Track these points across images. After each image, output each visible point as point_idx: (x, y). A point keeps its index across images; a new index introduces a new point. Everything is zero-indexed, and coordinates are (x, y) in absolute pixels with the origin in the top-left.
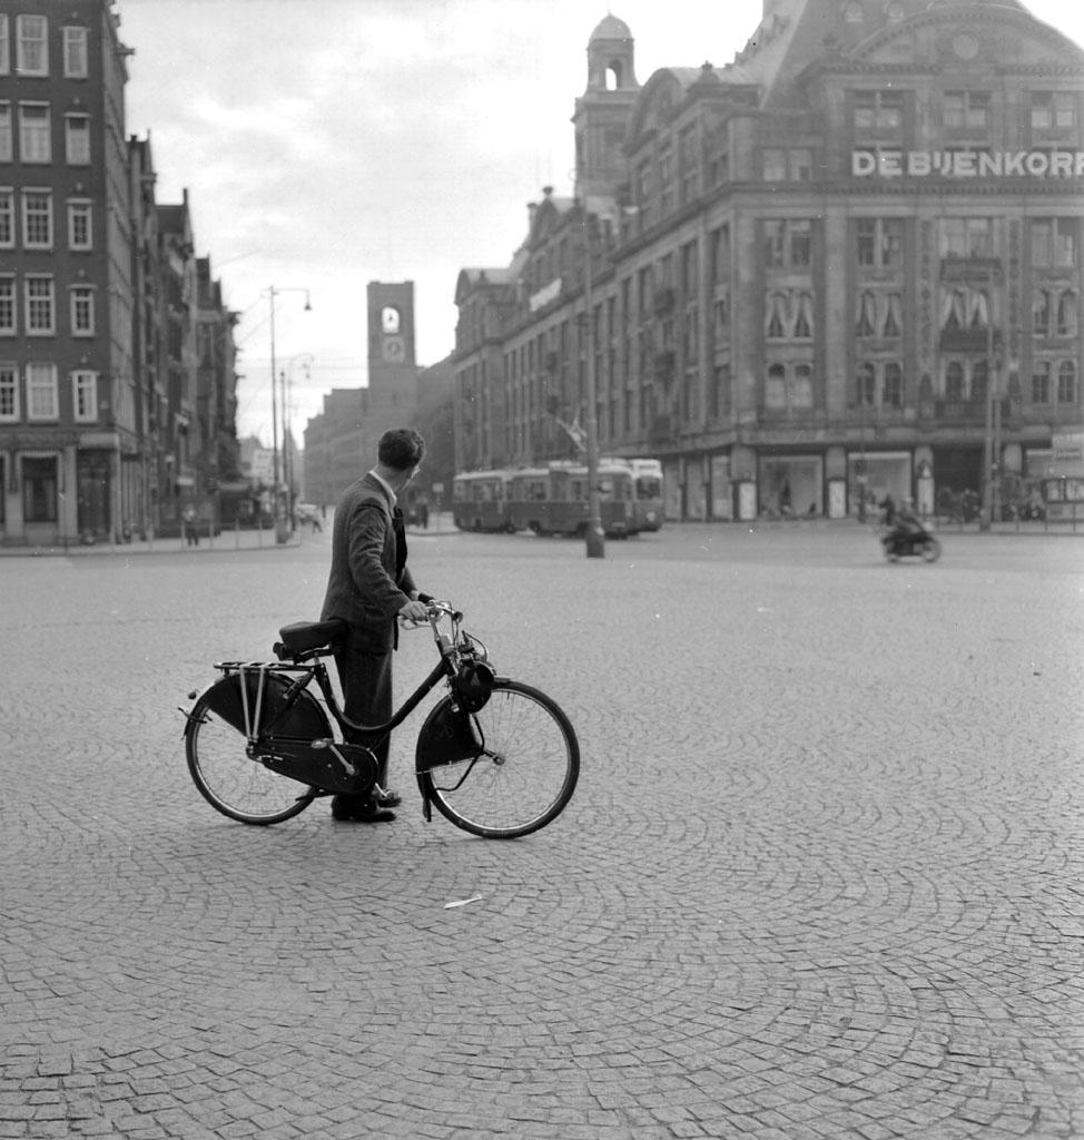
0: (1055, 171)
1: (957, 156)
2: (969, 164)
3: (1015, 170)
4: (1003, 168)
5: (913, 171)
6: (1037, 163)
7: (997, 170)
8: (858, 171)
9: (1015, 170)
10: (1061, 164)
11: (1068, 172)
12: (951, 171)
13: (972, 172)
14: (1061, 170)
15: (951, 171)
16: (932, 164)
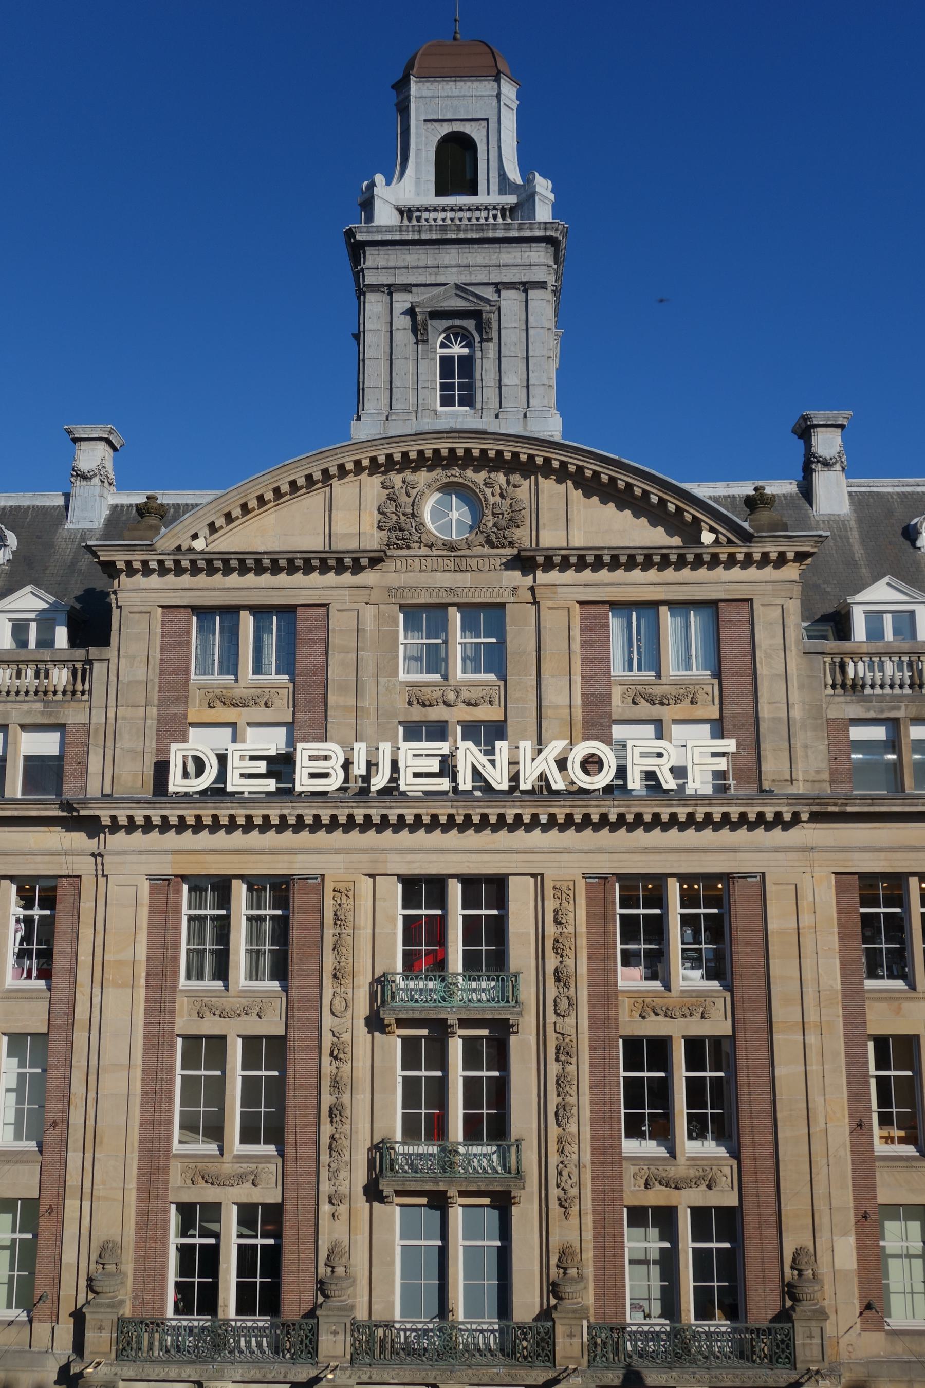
0: (635, 782)
1: (408, 749)
2: (434, 766)
3: (542, 777)
4: (515, 778)
5: (303, 783)
6: (591, 764)
7: (499, 779)
8: (176, 783)
9: (542, 777)
10: (651, 764)
11: (669, 782)
12: (394, 779)
13: (444, 784)
14: (650, 776)
15: (394, 779)
16: (347, 765)
